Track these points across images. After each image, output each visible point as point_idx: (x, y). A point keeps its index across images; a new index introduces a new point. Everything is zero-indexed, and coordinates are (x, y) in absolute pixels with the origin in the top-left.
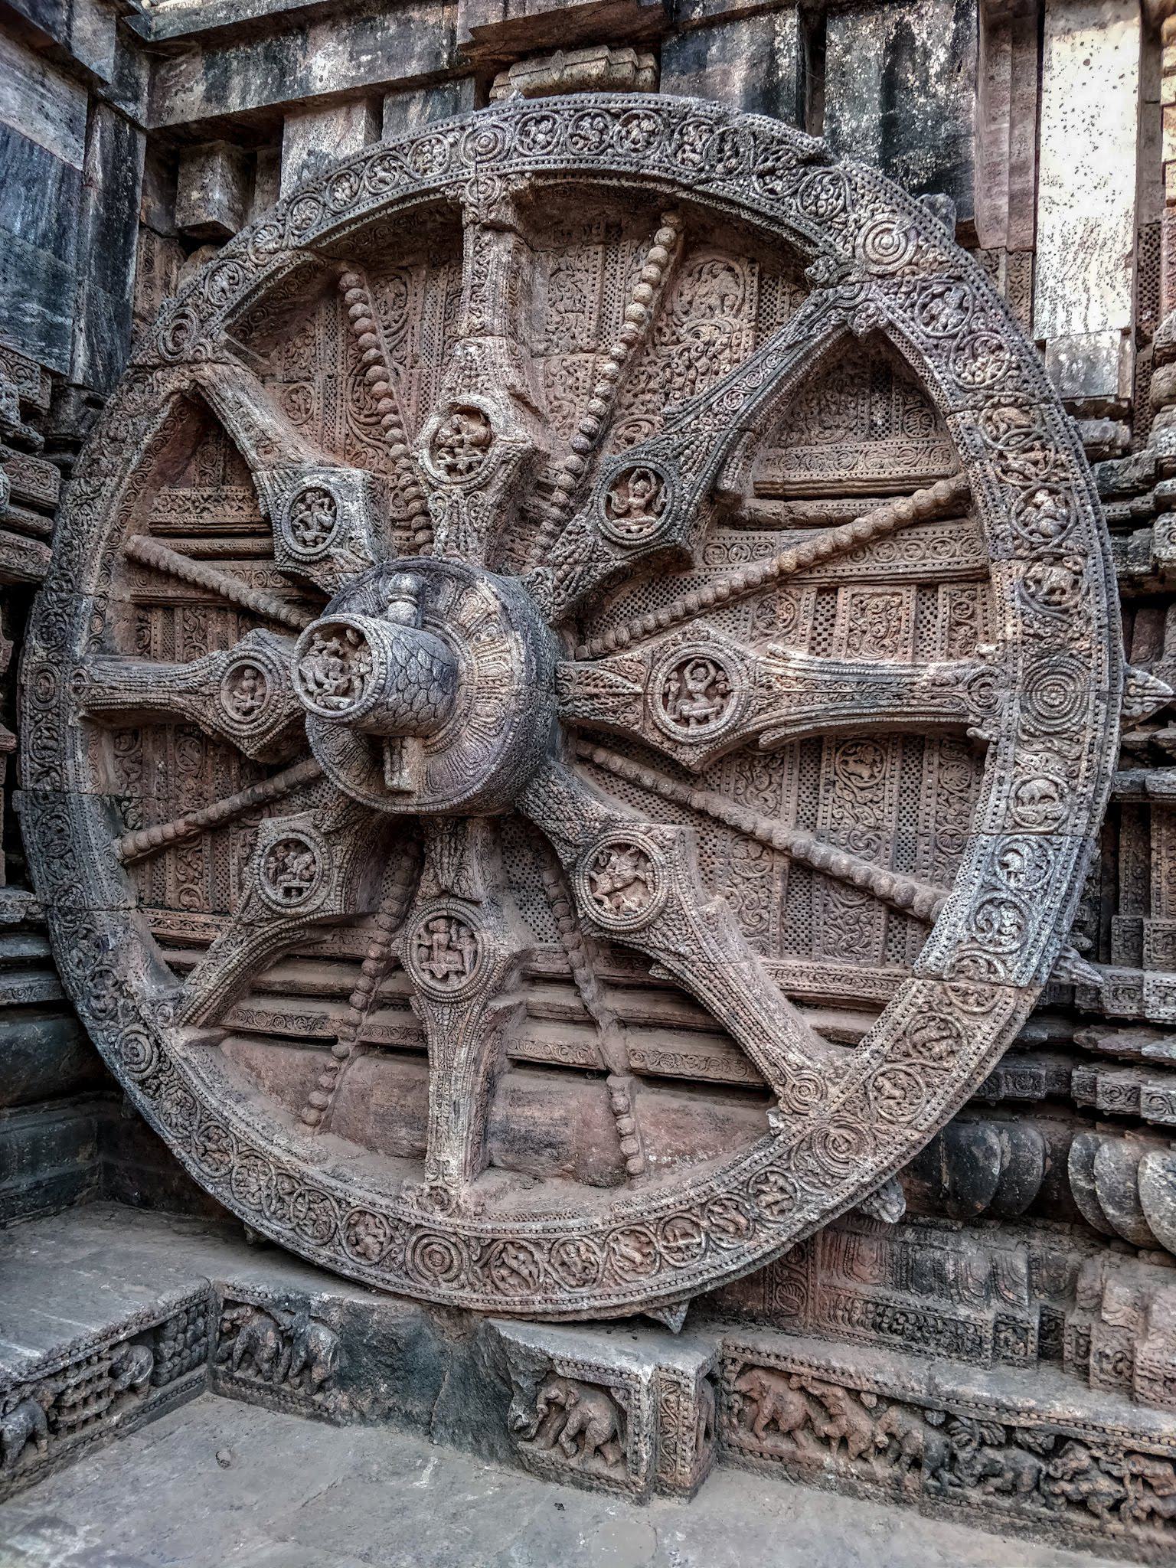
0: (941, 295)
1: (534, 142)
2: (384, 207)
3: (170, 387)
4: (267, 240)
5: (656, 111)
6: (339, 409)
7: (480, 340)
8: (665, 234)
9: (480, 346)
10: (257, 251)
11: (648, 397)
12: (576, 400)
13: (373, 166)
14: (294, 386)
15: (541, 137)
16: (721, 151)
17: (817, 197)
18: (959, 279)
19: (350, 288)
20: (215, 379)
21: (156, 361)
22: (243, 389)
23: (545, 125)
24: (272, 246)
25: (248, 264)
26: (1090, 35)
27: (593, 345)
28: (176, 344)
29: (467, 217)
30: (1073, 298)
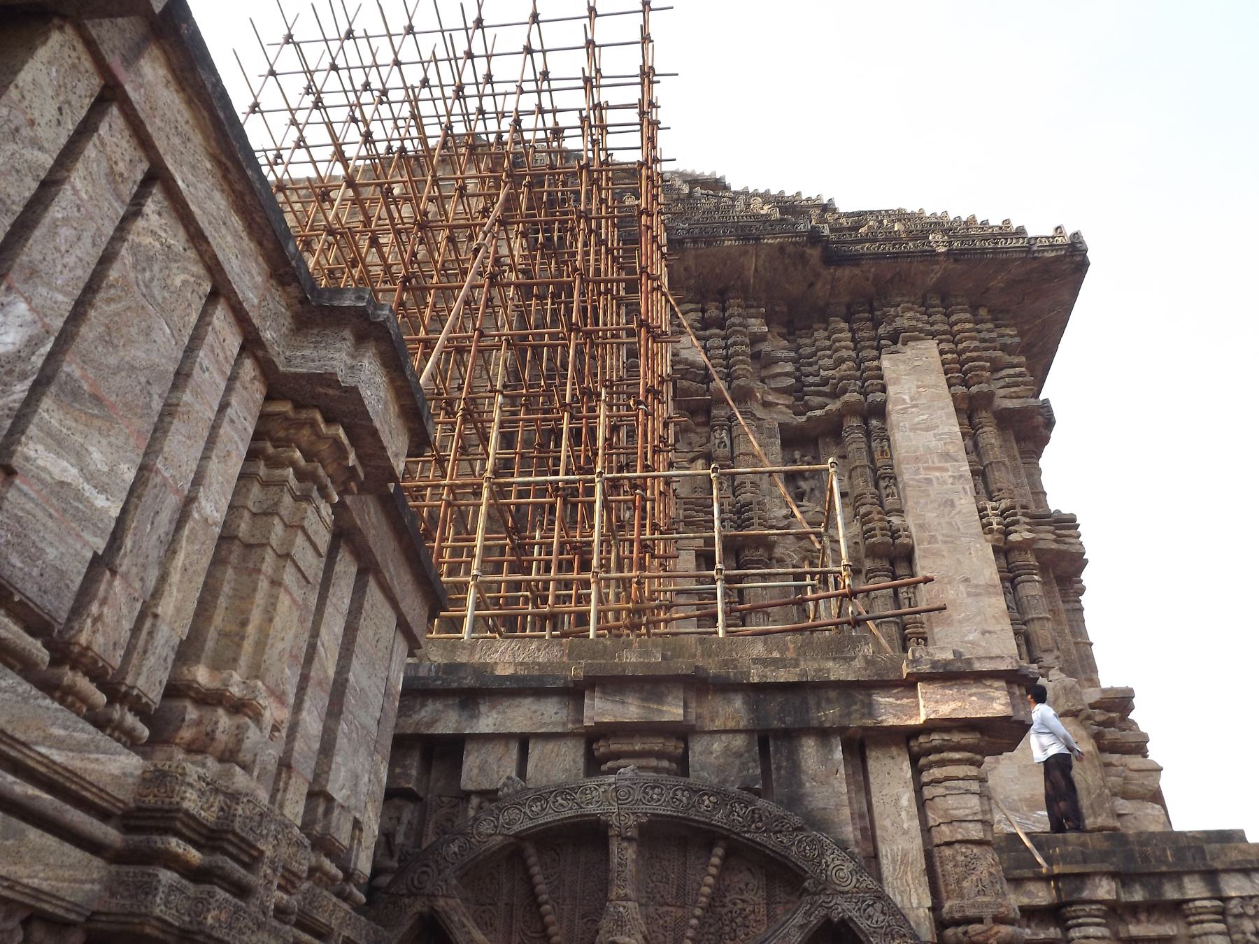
0: (872, 905)
1: (652, 798)
2: (562, 819)
3: (415, 910)
4: (486, 828)
5: (718, 793)
6: (514, 926)
7: (624, 903)
8: (719, 851)
9: (624, 907)
10: (479, 834)
11: (710, 936)
12: (667, 934)
13: (555, 796)
14: (484, 908)
15: (655, 796)
16: (753, 817)
17: (805, 848)
18: (879, 898)
19: (529, 857)
20: (447, 908)
21: (405, 891)
22: (464, 915)
23: (657, 790)
24: (490, 831)
25: (473, 840)
26: (889, 761)
27: (674, 902)
28: (420, 882)
29: (611, 833)
30: (902, 889)
